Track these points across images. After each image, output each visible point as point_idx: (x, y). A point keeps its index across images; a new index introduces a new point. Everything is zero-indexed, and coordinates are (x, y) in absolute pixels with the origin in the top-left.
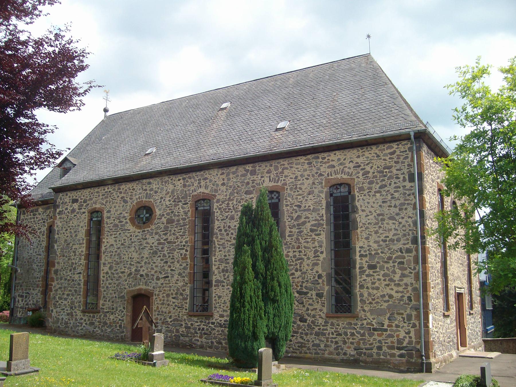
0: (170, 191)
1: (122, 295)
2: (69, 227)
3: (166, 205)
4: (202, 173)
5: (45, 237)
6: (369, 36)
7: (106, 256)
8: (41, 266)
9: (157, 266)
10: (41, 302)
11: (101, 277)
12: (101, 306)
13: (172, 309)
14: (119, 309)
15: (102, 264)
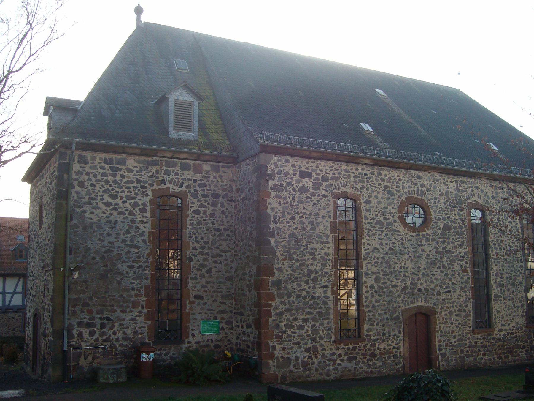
0: (444, 192)
1: (395, 315)
2: (298, 213)
3: (441, 208)
4: (473, 180)
5: (148, 214)
6: (459, 74)
7: (368, 263)
8: (140, 267)
9: (436, 279)
10: (146, 334)
11: (364, 293)
12: (366, 333)
13: (455, 328)
14: (393, 334)
15: (364, 275)
